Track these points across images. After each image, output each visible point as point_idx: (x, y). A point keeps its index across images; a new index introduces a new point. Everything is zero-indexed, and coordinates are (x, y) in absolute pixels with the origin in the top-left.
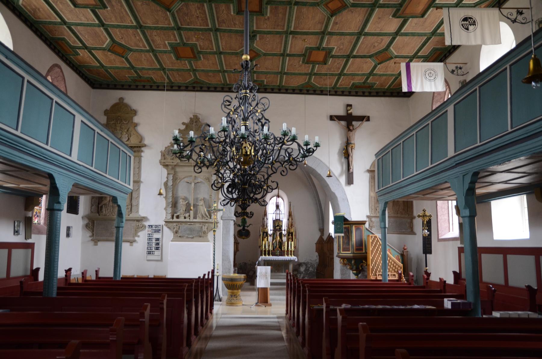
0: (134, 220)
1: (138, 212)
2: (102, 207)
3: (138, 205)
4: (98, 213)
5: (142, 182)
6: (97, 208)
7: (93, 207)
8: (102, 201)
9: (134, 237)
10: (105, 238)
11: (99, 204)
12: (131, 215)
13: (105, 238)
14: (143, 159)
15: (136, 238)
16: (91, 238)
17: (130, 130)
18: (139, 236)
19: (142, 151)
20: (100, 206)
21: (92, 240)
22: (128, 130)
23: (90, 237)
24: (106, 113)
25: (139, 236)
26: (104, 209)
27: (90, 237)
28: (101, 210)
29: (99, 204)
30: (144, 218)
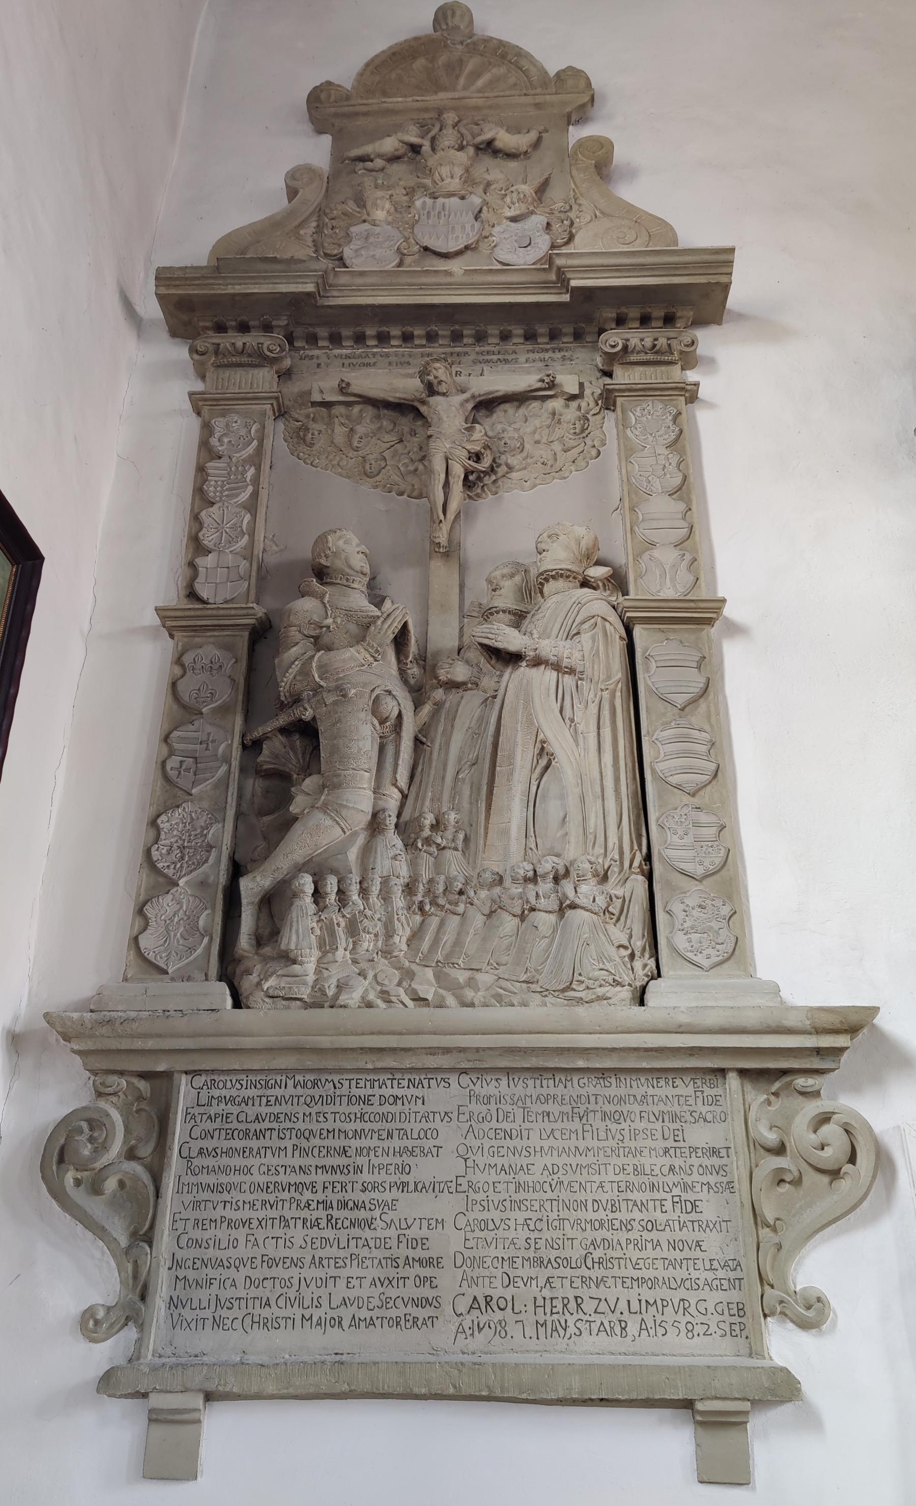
0: (708, 1066)
1: (736, 953)
2: (275, 903)
3: (724, 878)
4: (229, 969)
5: (735, 629)
6: (211, 919)
7: (165, 907)
8: (289, 823)
9: (742, 1324)
10: (315, 1343)
11: (237, 870)
12: (671, 998)
13: (315, 1343)
14: (704, 420)
15: (783, 1345)
16: (103, 1354)
17: (557, 195)
18: (811, 1314)
19: (689, 360)
20: (251, 887)
21: (108, 1383)
22: (542, 189)
23: (91, 1325)
24: (325, 108)
25: (811, 1314)
26: (303, 927)
27: (91, 1325)
28: (270, 932)
29: (237, 870)
30: (854, 1023)
